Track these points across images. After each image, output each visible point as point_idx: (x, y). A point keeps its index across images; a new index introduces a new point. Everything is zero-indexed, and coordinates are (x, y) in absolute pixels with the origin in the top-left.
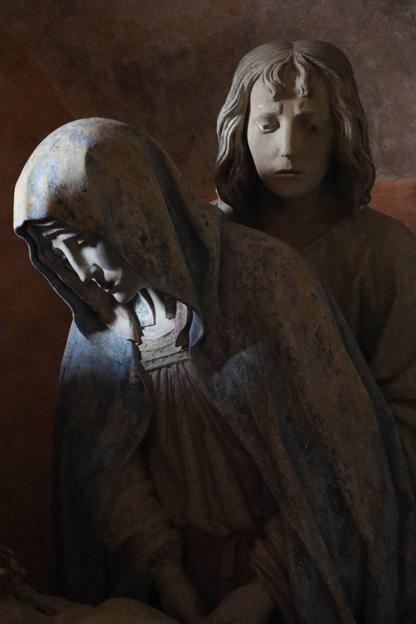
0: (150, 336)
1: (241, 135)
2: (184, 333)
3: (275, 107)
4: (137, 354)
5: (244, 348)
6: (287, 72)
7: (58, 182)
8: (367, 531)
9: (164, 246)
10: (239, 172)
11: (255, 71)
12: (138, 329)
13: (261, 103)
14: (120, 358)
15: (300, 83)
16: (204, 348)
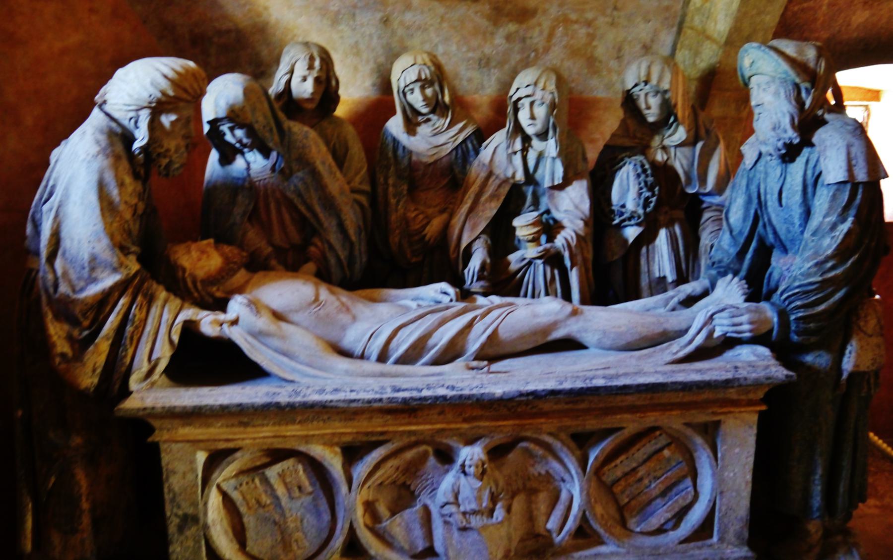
0: (253, 166)
1: (289, 82)
2: (275, 165)
3: (306, 73)
4: (249, 175)
5: (299, 170)
6: (312, 59)
7: (231, 102)
8: (354, 238)
9: (271, 130)
10: (285, 98)
11: (297, 57)
12: (248, 164)
13: (300, 70)
14: (241, 176)
15: (317, 63)
16: (283, 172)
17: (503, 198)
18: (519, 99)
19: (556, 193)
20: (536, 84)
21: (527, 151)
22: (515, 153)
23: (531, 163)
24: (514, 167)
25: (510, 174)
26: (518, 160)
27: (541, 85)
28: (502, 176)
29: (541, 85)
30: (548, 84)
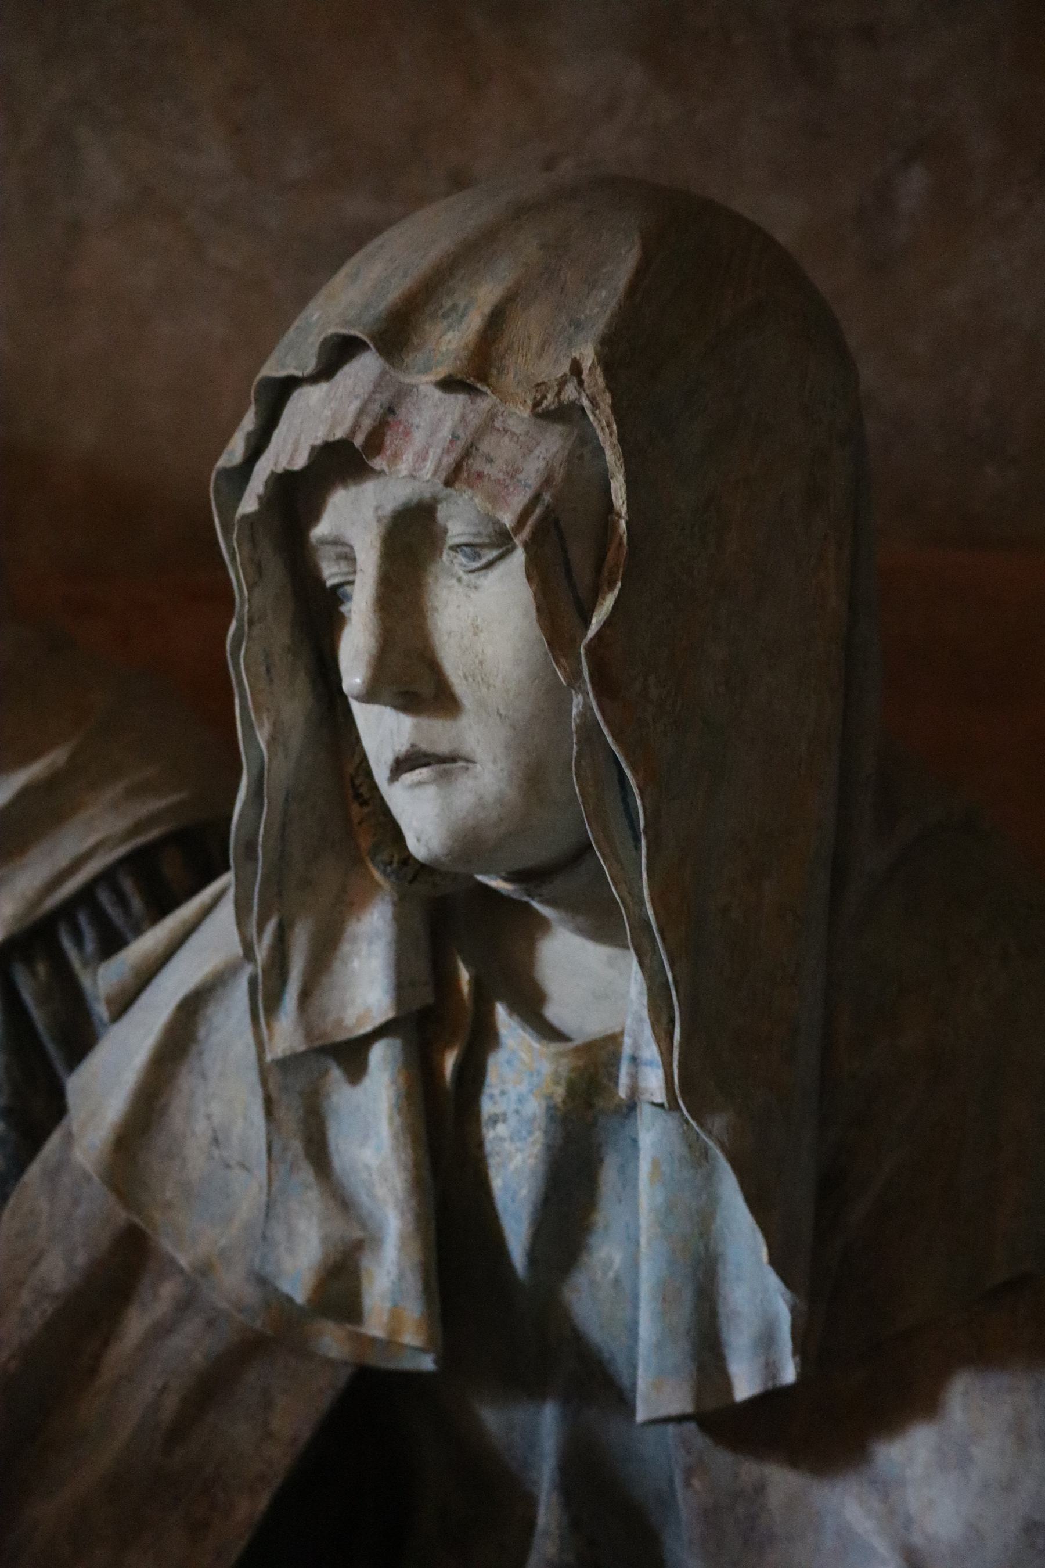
17: (249, 1508)
18: (297, 497)
19: (781, 1481)
20: (395, 334)
21: (482, 1040)
22: (352, 1055)
23: (514, 1163)
24: (341, 1200)
25: (298, 1270)
26: (371, 1126)
27: (450, 341)
28: (232, 1284)
29: (450, 341)
30: (528, 325)
